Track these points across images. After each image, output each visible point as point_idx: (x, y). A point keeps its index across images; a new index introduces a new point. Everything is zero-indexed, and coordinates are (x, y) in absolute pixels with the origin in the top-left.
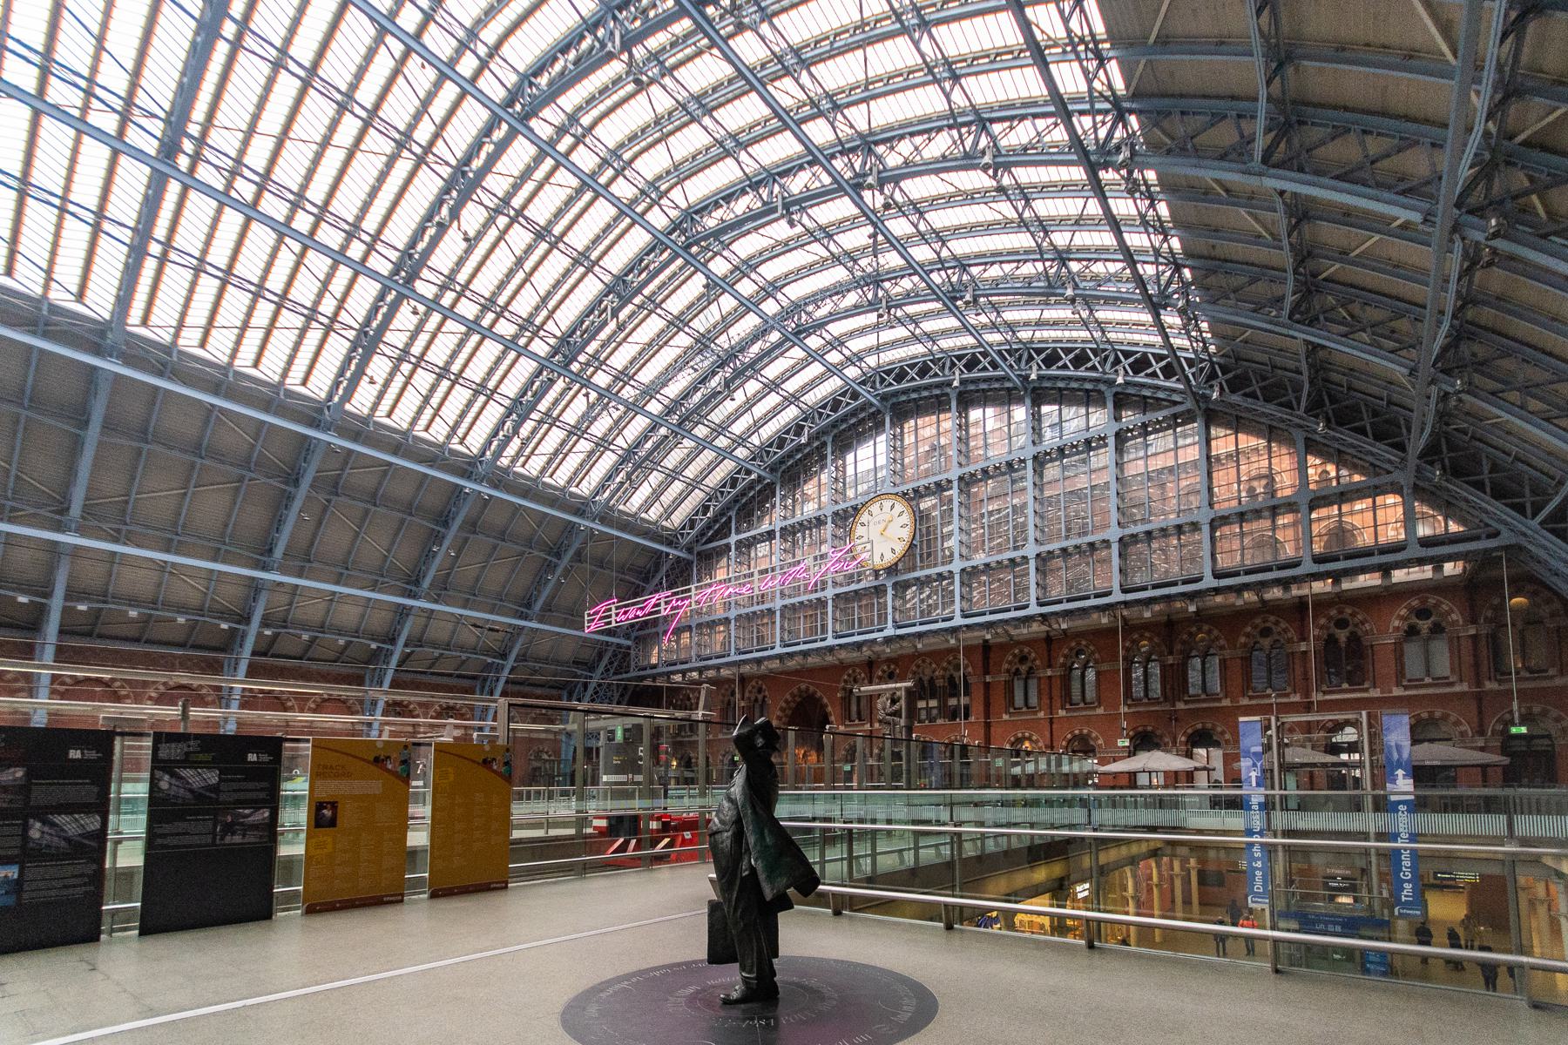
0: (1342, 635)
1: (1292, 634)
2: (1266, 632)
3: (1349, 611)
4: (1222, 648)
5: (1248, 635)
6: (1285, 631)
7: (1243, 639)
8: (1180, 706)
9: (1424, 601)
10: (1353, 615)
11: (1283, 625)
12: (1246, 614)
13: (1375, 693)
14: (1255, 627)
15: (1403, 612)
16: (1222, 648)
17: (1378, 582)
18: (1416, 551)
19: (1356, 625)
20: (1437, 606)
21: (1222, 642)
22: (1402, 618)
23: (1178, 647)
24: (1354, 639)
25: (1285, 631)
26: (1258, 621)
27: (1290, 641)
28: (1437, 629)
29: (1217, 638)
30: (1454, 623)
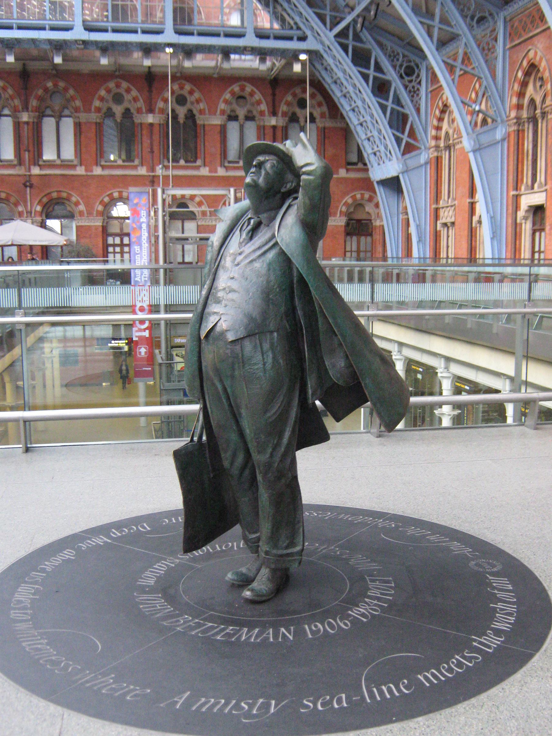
0: (182, 112)
1: (141, 104)
2: (118, 99)
3: (188, 87)
4: (77, 110)
5: (102, 99)
6: (135, 99)
7: (97, 103)
8: (36, 171)
9: (243, 89)
10: (191, 92)
11: (134, 93)
12: (102, 77)
13: (204, 171)
14: (109, 91)
15: (227, 96)
16: (77, 110)
17: (212, 64)
18: (250, 40)
19: (192, 103)
20: (252, 94)
21: (78, 103)
22: (226, 102)
23: (34, 103)
24: (191, 116)
25: (135, 99)
26: (111, 85)
27: (139, 111)
28: (249, 118)
29: (73, 98)
30: (262, 113)
